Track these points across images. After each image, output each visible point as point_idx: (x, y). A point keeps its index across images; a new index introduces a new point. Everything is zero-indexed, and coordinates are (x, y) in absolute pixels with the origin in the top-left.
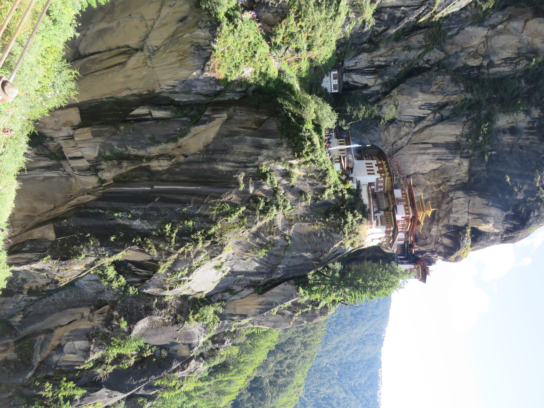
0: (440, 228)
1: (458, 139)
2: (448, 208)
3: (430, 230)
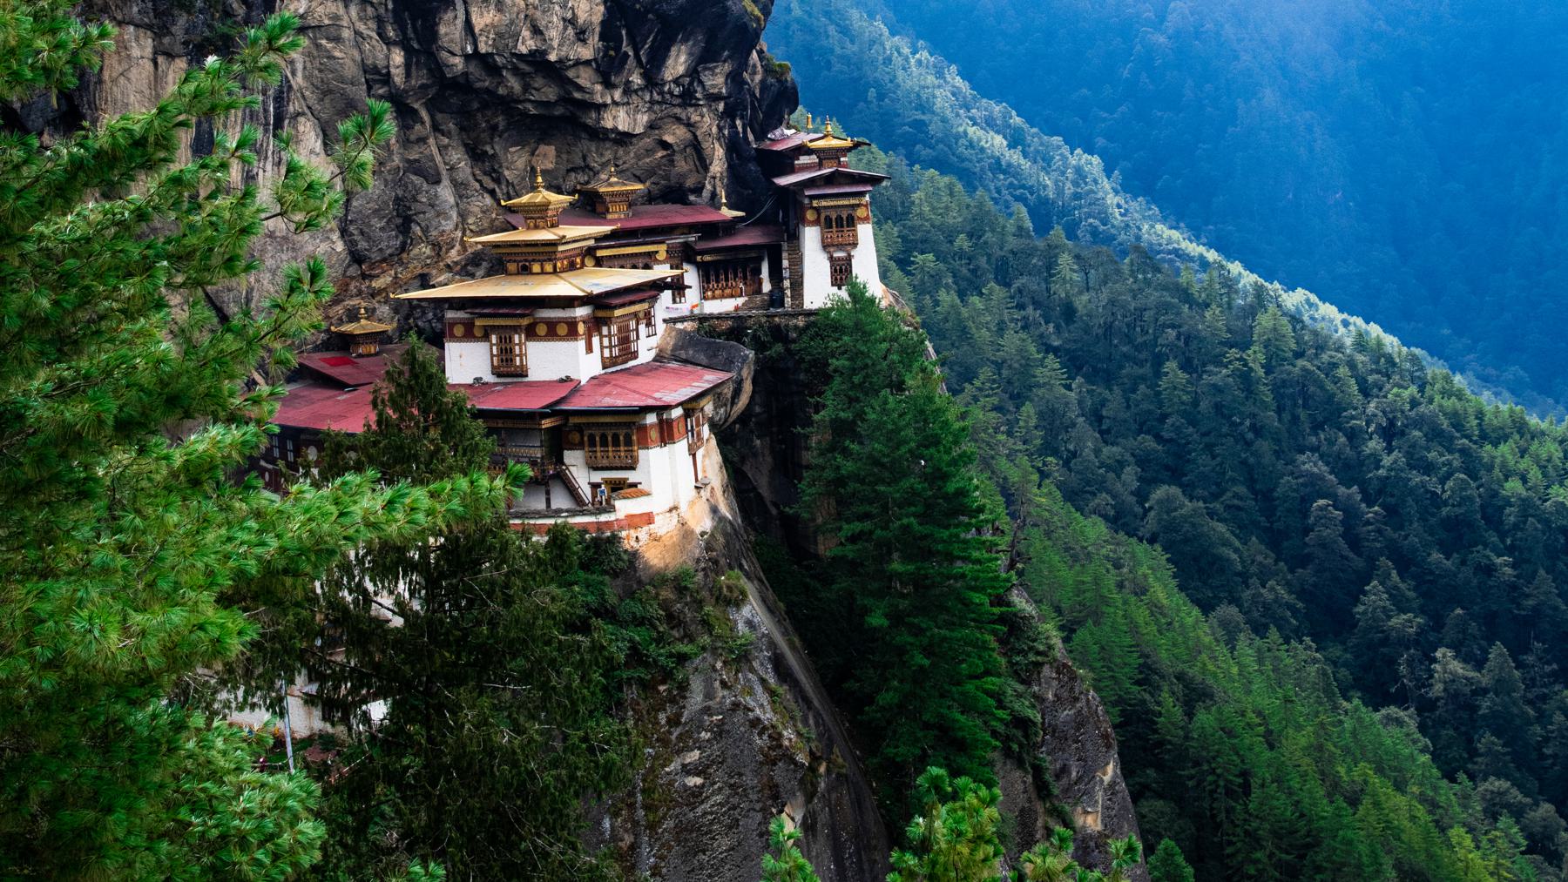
0: (617, 95)
1: (179, 48)
2: (516, 71)
3: (624, 139)
